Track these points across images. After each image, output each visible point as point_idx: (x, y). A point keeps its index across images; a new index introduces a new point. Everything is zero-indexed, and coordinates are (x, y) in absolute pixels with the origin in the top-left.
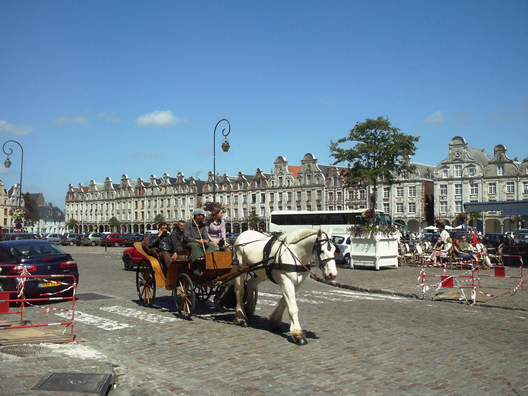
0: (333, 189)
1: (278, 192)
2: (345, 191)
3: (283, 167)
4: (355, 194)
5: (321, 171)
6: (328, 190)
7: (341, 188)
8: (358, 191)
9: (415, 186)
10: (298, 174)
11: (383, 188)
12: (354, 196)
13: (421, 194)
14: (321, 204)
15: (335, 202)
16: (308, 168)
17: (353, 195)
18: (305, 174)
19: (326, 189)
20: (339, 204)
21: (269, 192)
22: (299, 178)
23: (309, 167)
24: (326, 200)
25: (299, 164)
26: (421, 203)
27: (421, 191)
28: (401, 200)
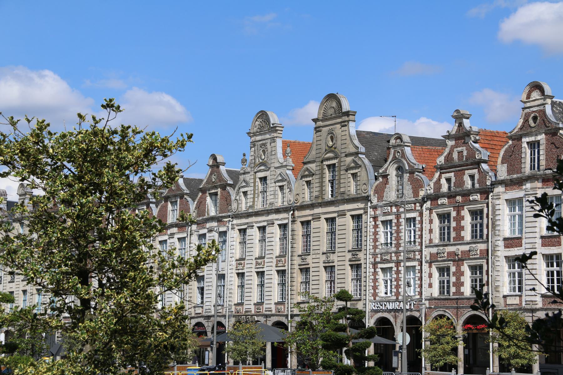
0: (394, 210)
1: (256, 225)
2: (426, 213)
4: (453, 224)
5: (363, 149)
6: (378, 212)
7: (415, 204)
8: (465, 213)
10: (305, 163)
12: (452, 229)
14: (362, 262)
15: (397, 253)
16: (331, 143)
17: (449, 228)
18: (322, 162)
19: (375, 208)
20: (409, 259)
21: (237, 228)
22: (306, 176)
23: (332, 139)
24: (375, 247)
25: (308, 137)
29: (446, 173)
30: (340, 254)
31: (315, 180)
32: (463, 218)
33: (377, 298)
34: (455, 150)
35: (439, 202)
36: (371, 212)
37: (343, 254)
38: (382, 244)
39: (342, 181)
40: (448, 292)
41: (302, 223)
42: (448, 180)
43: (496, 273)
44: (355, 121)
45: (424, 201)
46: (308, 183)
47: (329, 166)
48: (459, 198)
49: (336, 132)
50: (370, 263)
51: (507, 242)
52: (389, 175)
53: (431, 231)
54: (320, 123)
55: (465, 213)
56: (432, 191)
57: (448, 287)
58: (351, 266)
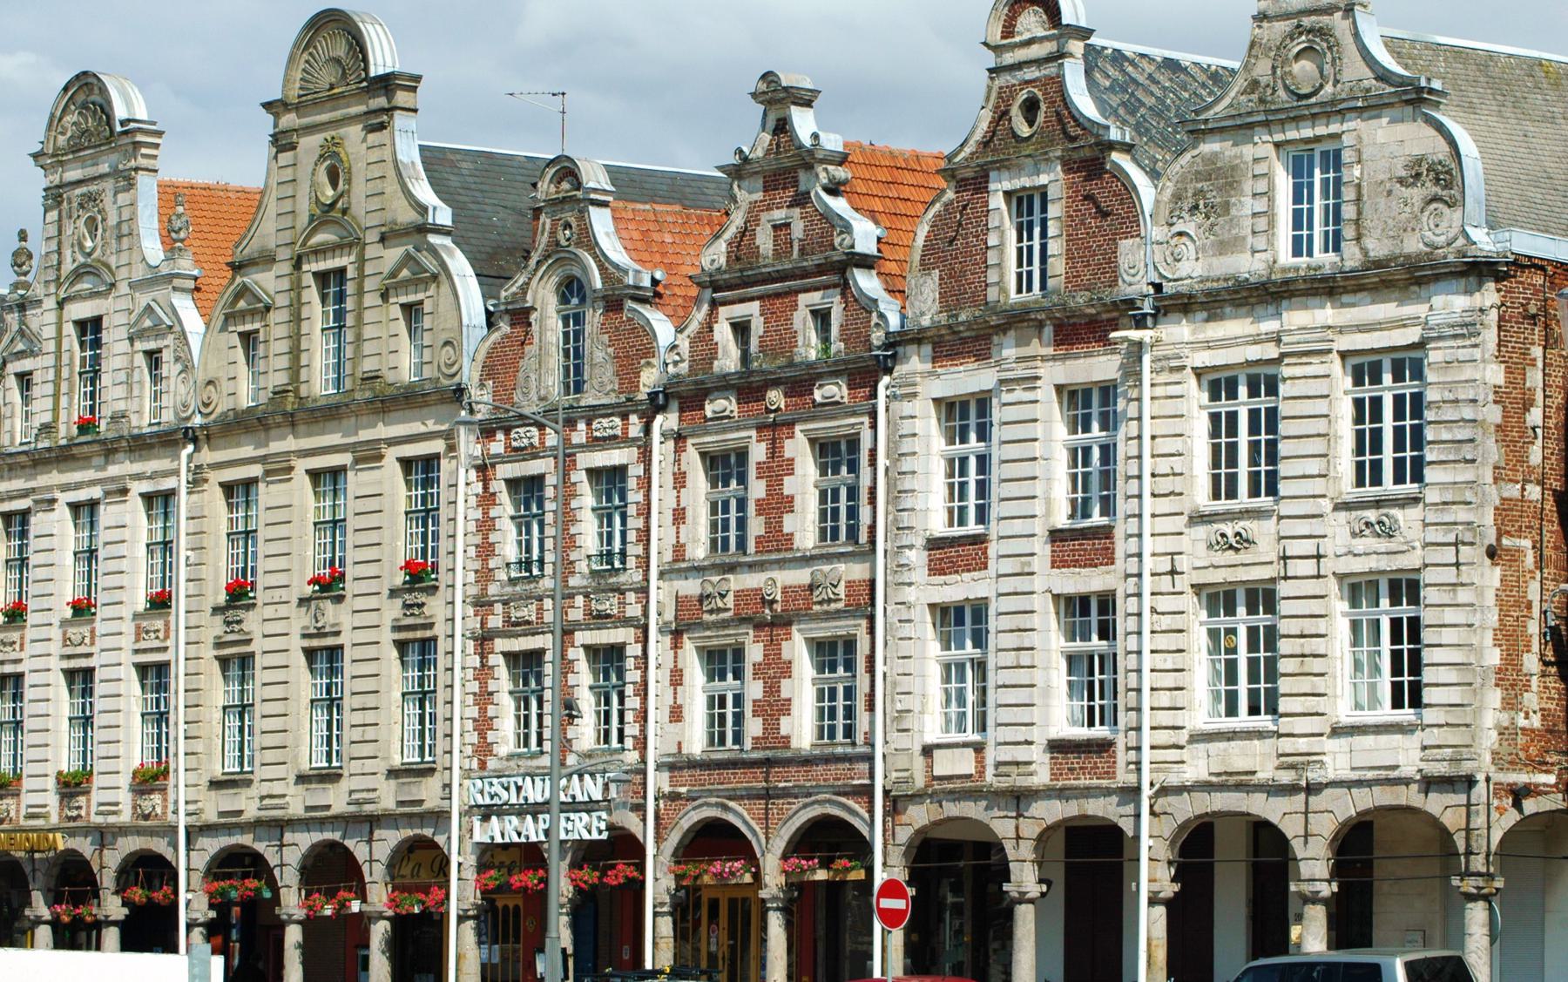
2: (661, 451)
3: (108, 198)
4: (757, 489)
5: (444, 216)
6: (497, 446)
7: (625, 417)
8: (798, 447)
9: (1421, 345)
10: (237, 267)
11: (1045, 392)
12: (751, 508)
13: (1492, 451)
14: (440, 630)
16: (330, 192)
17: (742, 504)
22: (242, 316)
24: (485, 575)
26: (1492, 577)
27: (1494, 414)
28: (1244, 541)
29: (732, 302)
30: (361, 603)
31: (276, 328)
32: (789, 467)
33: (492, 764)
34: (764, 217)
35: (709, 409)
36: (469, 445)
37: (372, 602)
38: (508, 565)
39: (368, 332)
40: (738, 738)
41: (228, 489)
42: (741, 329)
43: (901, 666)
44: (415, 111)
45: (656, 404)
46: (248, 339)
47: (322, 278)
48: (776, 397)
49: (350, 150)
50: (468, 634)
51: (938, 554)
52: (533, 309)
53: (679, 516)
54: (289, 120)
55: (798, 447)
56: (684, 368)
57: (739, 719)
58: (401, 646)
